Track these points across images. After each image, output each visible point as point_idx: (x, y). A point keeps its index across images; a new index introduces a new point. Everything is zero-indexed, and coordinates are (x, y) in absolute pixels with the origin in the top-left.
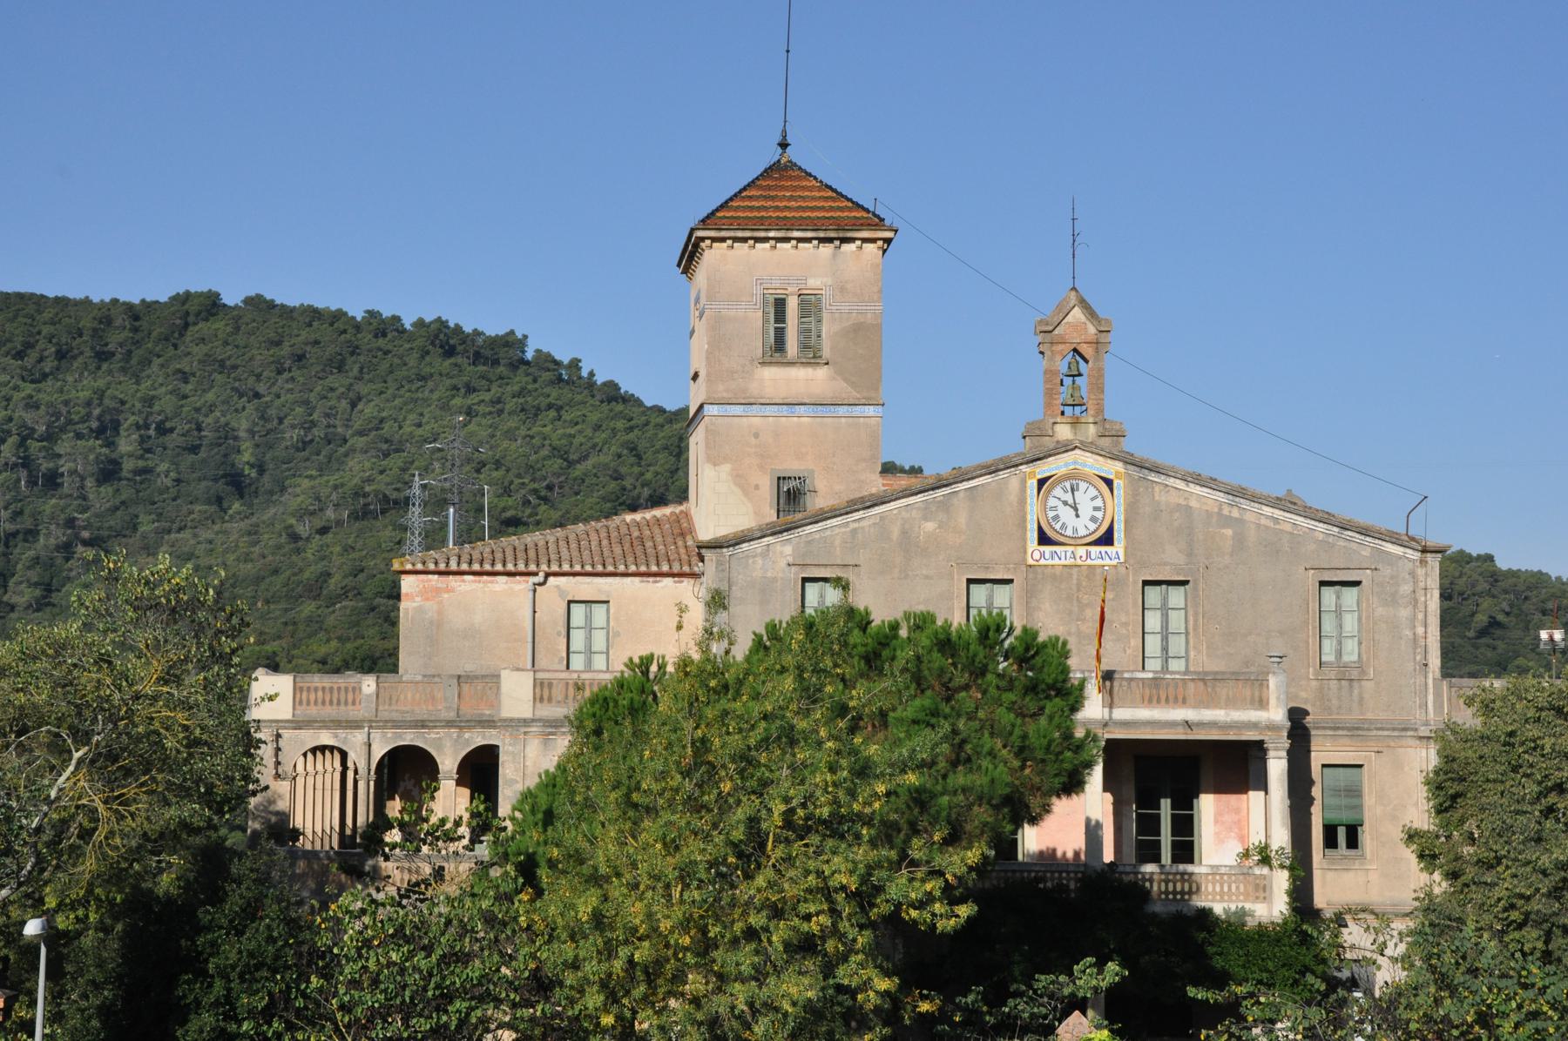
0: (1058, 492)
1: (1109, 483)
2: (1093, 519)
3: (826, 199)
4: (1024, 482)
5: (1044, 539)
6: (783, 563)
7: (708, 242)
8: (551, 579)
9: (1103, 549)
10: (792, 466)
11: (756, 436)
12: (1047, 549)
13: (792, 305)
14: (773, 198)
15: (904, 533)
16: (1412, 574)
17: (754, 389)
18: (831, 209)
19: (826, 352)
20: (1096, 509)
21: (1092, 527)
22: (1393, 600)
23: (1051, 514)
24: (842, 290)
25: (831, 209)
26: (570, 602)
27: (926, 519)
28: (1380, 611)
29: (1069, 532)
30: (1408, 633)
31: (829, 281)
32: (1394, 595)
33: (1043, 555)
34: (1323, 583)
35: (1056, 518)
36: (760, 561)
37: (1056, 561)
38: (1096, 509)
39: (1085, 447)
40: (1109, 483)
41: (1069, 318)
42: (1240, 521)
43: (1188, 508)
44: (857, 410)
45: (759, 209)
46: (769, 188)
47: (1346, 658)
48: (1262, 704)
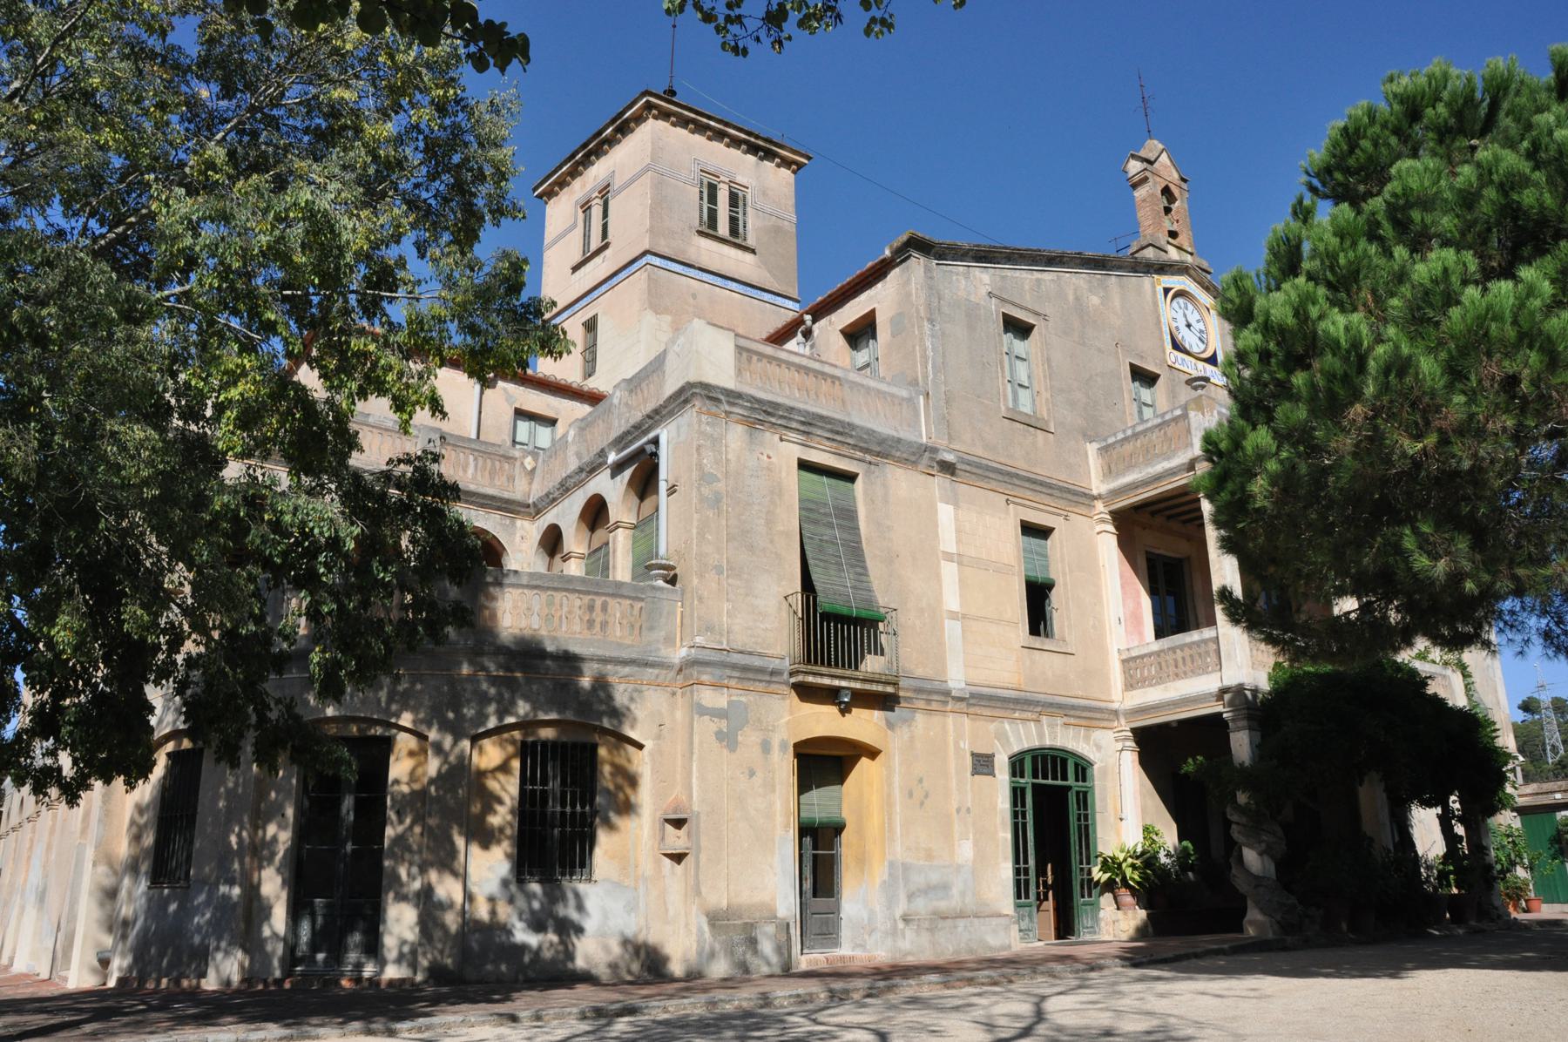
6: (983, 291)
7: (655, 112)
11: (694, 296)
15: (1077, 299)
17: (691, 256)
24: (764, 194)
44: (779, 301)
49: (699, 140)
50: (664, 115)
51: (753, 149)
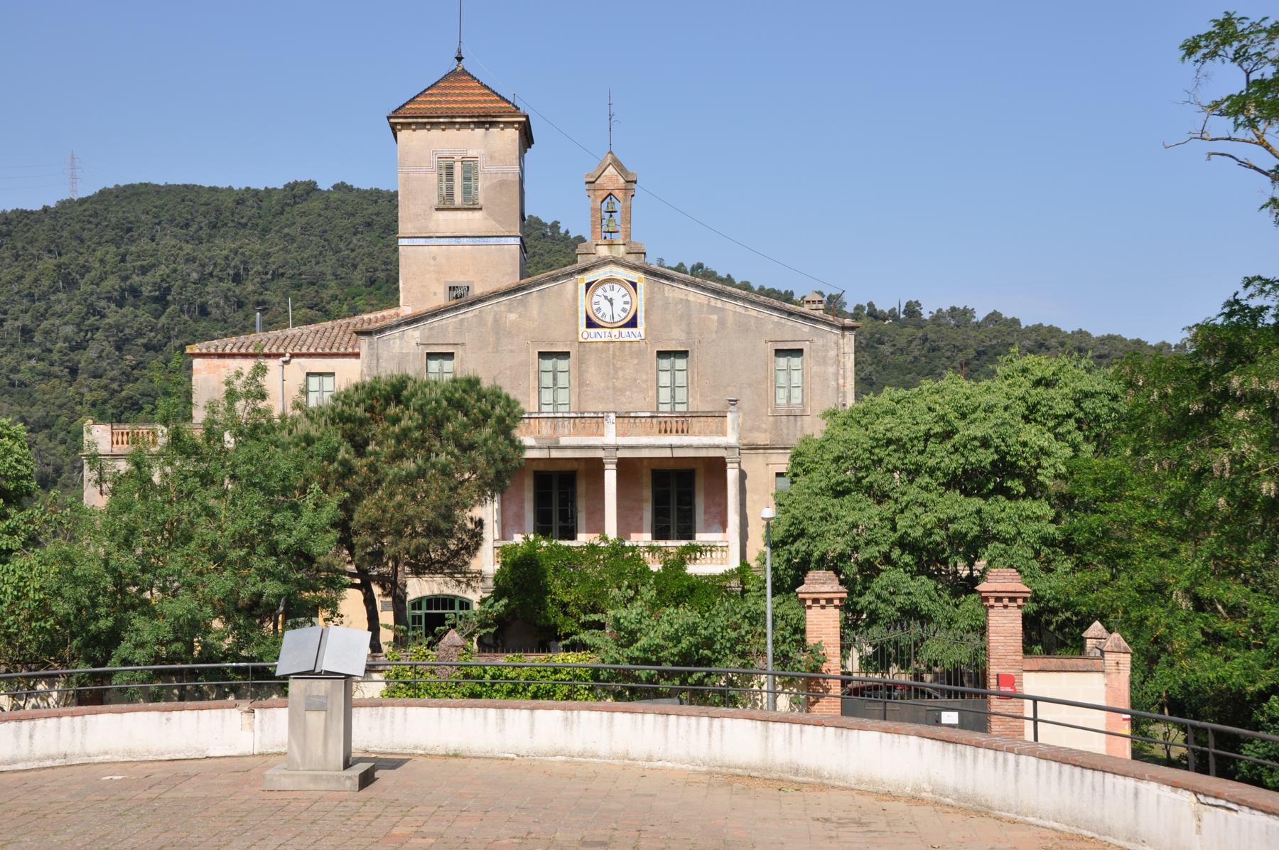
0: (600, 291)
1: (634, 285)
2: (624, 310)
3: (483, 95)
4: (576, 285)
5: (590, 324)
6: (414, 343)
8: (294, 361)
9: (630, 330)
10: (459, 279)
11: (434, 258)
12: (593, 331)
13: (458, 168)
14: (446, 95)
15: (496, 321)
16: (837, 343)
18: (485, 101)
19: (481, 201)
20: (626, 303)
21: (623, 315)
22: (823, 361)
23: (595, 307)
24: (492, 157)
25: (485, 101)
26: (308, 374)
27: (510, 311)
28: (815, 369)
29: (608, 319)
30: (833, 383)
31: (482, 151)
32: (824, 358)
33: (589, 335)
34: (777, 351)
35: (599, 309)
36: (398, 341)
37: (599, 339)
38: (626, 303)
39: (615, 262)
40: (634, 285)
41: (606, 173)
42: (722, 309)
43: (688, 301)
44: (503, 241)
45: (435, 102)
46: (446, 88)
47: (793, 401)
48: (724, 434)
49: (436, 133)
50: (407, 126)
51: (479, 125)
